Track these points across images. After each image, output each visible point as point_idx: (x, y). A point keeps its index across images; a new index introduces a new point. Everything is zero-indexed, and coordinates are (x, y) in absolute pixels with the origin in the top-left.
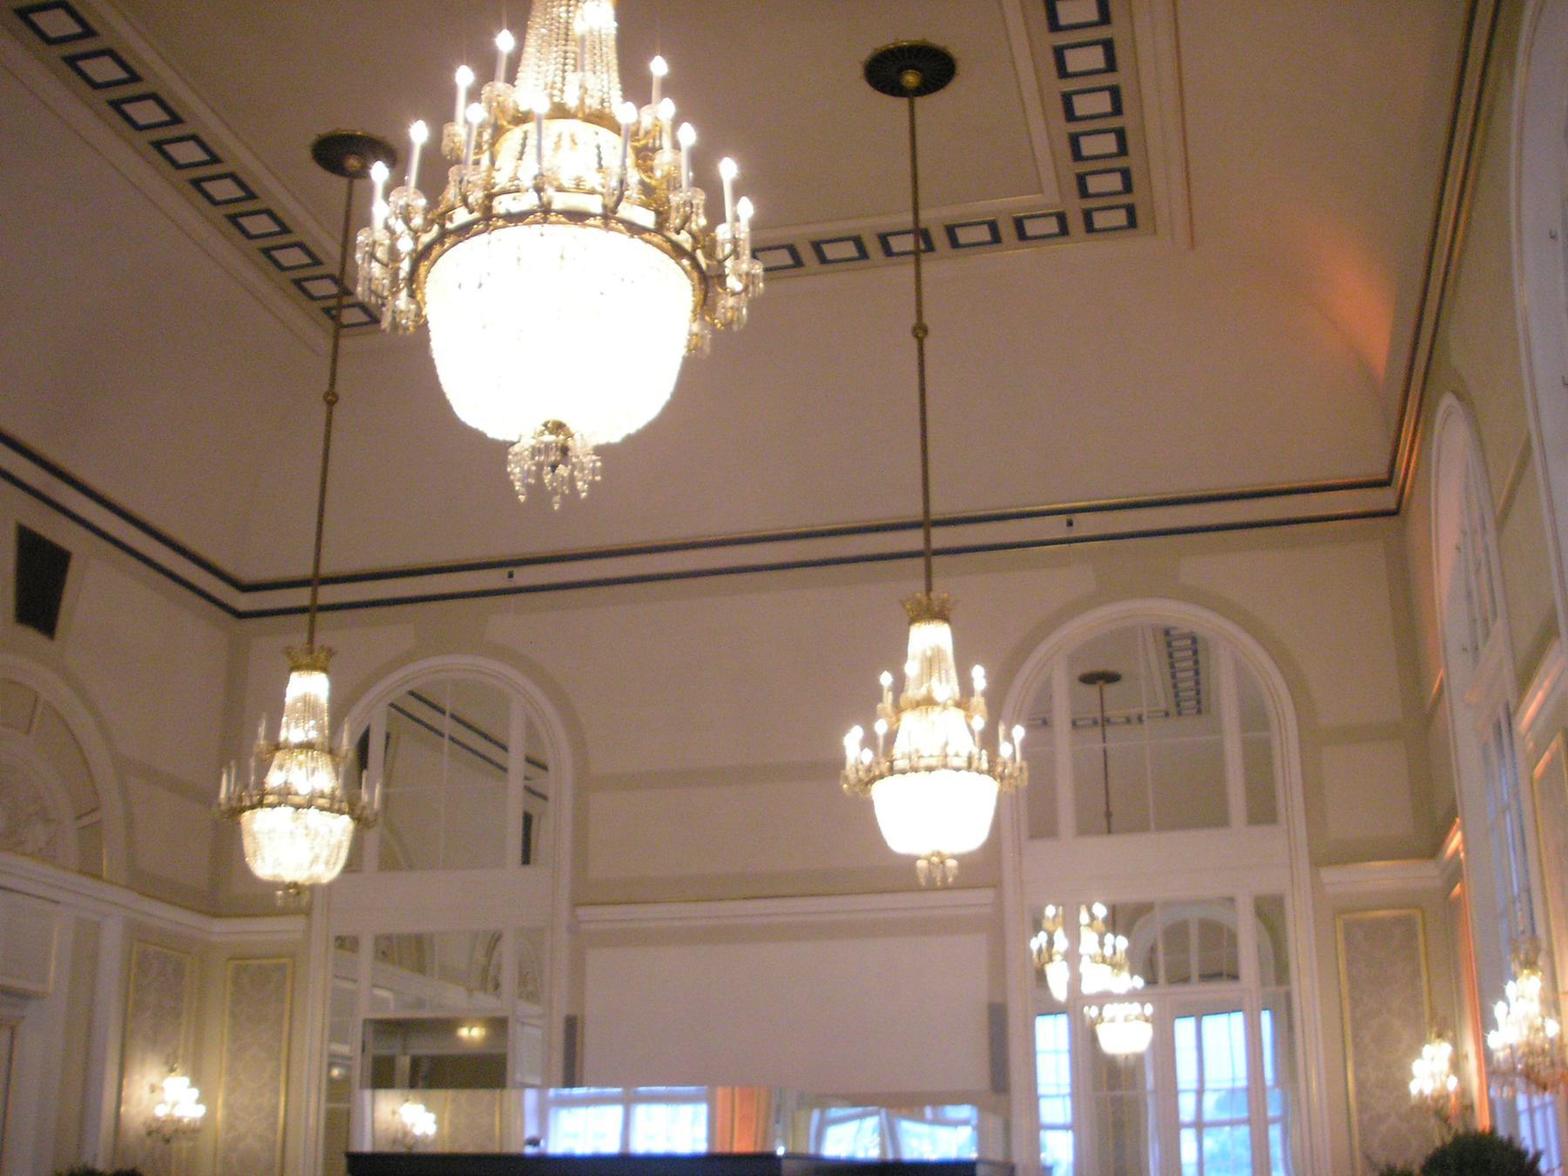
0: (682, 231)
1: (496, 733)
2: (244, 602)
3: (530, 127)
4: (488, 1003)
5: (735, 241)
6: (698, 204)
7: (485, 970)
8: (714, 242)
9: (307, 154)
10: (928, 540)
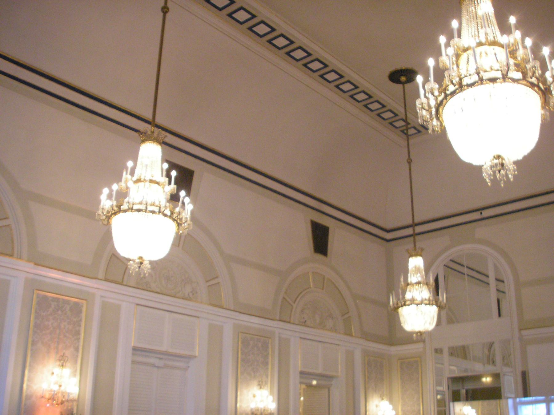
1: (482, 271)
2: (389, 236)
4: (490, 368)
7: (489, 357)
9: (387, 79)
10: (414, 230)
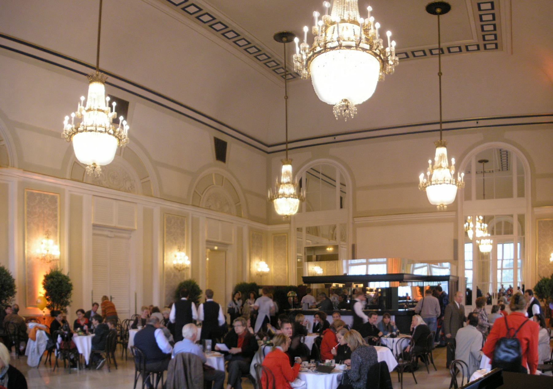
0: (377, 50)
3: (336, 25)
5: (391, 52)
6: (381, 43)
8: (385, 52)
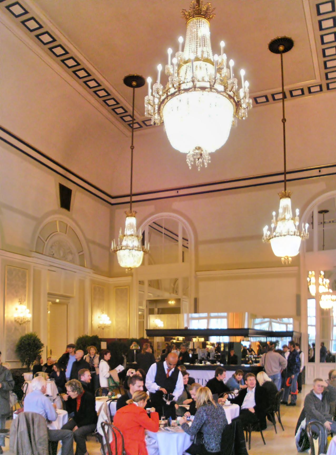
5: (245, 93)
6: (235, 83)
